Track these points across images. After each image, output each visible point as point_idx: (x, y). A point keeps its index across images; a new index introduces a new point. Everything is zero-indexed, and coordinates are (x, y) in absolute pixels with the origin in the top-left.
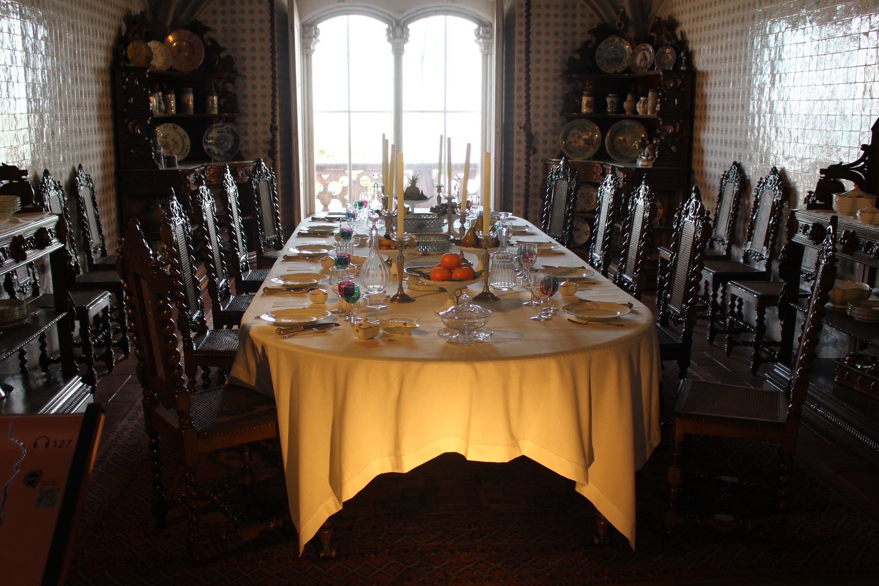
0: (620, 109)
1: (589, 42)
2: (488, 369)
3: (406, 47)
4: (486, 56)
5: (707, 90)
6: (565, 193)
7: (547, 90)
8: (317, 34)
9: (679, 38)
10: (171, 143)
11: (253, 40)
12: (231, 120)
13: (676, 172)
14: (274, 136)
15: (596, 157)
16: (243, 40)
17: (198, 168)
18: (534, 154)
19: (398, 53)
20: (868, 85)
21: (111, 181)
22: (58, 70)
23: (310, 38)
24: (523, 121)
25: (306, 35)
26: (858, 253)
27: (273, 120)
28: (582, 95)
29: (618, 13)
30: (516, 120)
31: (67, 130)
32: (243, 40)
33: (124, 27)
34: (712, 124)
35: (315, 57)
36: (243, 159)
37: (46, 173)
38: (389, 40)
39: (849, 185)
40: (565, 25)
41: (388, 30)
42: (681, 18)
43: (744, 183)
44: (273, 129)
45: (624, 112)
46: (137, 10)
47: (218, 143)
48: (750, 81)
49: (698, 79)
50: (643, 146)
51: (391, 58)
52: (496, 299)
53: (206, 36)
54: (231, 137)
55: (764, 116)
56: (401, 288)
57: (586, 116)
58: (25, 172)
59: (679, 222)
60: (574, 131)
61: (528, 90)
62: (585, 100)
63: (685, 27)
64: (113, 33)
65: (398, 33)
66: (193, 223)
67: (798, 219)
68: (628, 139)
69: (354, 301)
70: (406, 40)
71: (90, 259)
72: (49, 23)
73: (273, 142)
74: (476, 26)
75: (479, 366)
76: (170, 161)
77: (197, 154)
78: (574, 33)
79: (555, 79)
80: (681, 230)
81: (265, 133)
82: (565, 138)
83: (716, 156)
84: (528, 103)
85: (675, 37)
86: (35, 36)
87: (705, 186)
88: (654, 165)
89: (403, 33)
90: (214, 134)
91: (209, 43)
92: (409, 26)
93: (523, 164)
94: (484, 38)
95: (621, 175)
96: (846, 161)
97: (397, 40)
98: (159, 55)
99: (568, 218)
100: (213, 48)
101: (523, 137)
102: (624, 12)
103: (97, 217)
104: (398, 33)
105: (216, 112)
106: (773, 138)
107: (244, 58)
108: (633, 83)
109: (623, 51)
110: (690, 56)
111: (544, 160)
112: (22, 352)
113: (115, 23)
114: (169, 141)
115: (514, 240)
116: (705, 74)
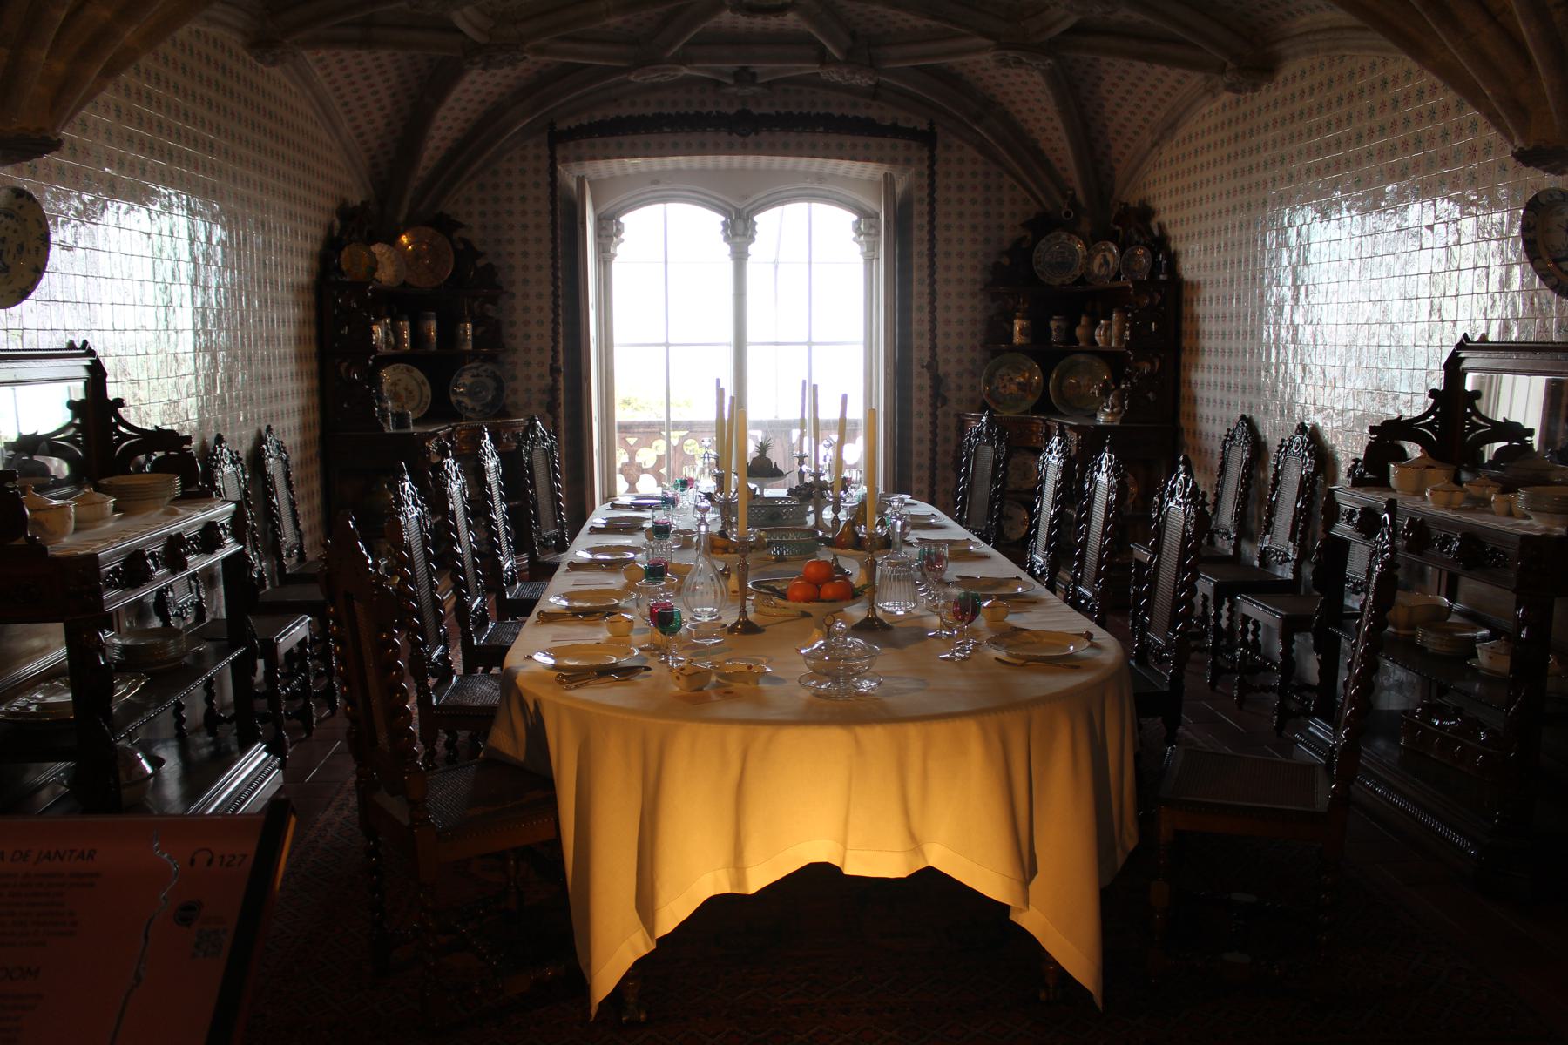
0: (1070, 338)
2: (874, 737)
3: (752, 248)
4: (869, 261)
5: (1200, 309)
6: (989, 465)
7: (961, 311)
8: (619, 231)
9: (1156, 232)
10: (403, 393)
11: (525, 240)
12: (491, 358)
13: (1155, 430)
14: (555, 381)
15: (1036, 409)
16: (511, 241)
17: (441, 429)
18: (943, 404)
19: (740, 257)
20: (1436, 301)
21: (314, 450)
22: (240, 288)
23: (610, 237)
24: (926, 356)
25: (603, 233)
26: (1429, 551)
27: (555, 359)
28: (1015, 317)
30: (915, 355)
31: (250, 376)
32: (511, 241)
33: (337, 223)
34: (1206, 360)
35: (617, 267)
36: (509, 416)
37: (219, 439)
38: (727, 239)
39: (1413, 450)
40: (987, 214)
41: (724, 224)
42: (1159, 204)
43: (1257, 447)
44: (554, 371)
45: (1077, 342)
46: (356, 199)
47: (471, 393)
48: (1262, 296)
49: (1186, 294)
50: (1105, 392)
51: (728, 266)
52: (887, 628)
53: (456, 236)
54: (491, 384)
55: (1285, 348)
56: (743, 613)
57: (1020, 349)
58: (188, 440)
59: (1161, 509)
60: (1002, 371)
61: (933, 310)
62: (1017, 325)
63: (1164, 217)
64: (320, 233)
65: (739, 230)
66: (433, 512)
67: (1340, 501)
68: (1084, 382)
69: (674, 631)
70: (752, 239)
71: (282, 567)
72: (229, 221)
73: (553, 390)
74: (855, 218)
75: (859, 730)
76: (401, 420)
77: (442, 409)
78: (1001, 227)
79: (974, 295)
80: (1165, 521)
81: (541, 377)
82: (989, 382)
83: (1215, 409)
84: (933, 330)
85: (1150, 231)
86: (209, 239)
87: (1199, 451)
89: (746, 228)
90: (467, 379)
91: (461, 246)
92: (756, 218)
93: (927, 419)
94: (867, 234)
95: (1073, 437)
96: (1408, 414)
97: (738, 240)
98: (389, 261)
99: (996, 501)
100: (467, 253)
101: (927, 382)
102: (1074, 195)
103: (292, 504)
104: (739, 230)
105: (470, 347)
106: (1299, 381)
107: (512, 267)
108: (1089, 300)
109: (1073, 252)
110: (1173, 259)
111: (958, 415)
112: (179, 707)
113: (324, 219)
114: (401, 390)
115: (913, 536)
116: (1195, 286)
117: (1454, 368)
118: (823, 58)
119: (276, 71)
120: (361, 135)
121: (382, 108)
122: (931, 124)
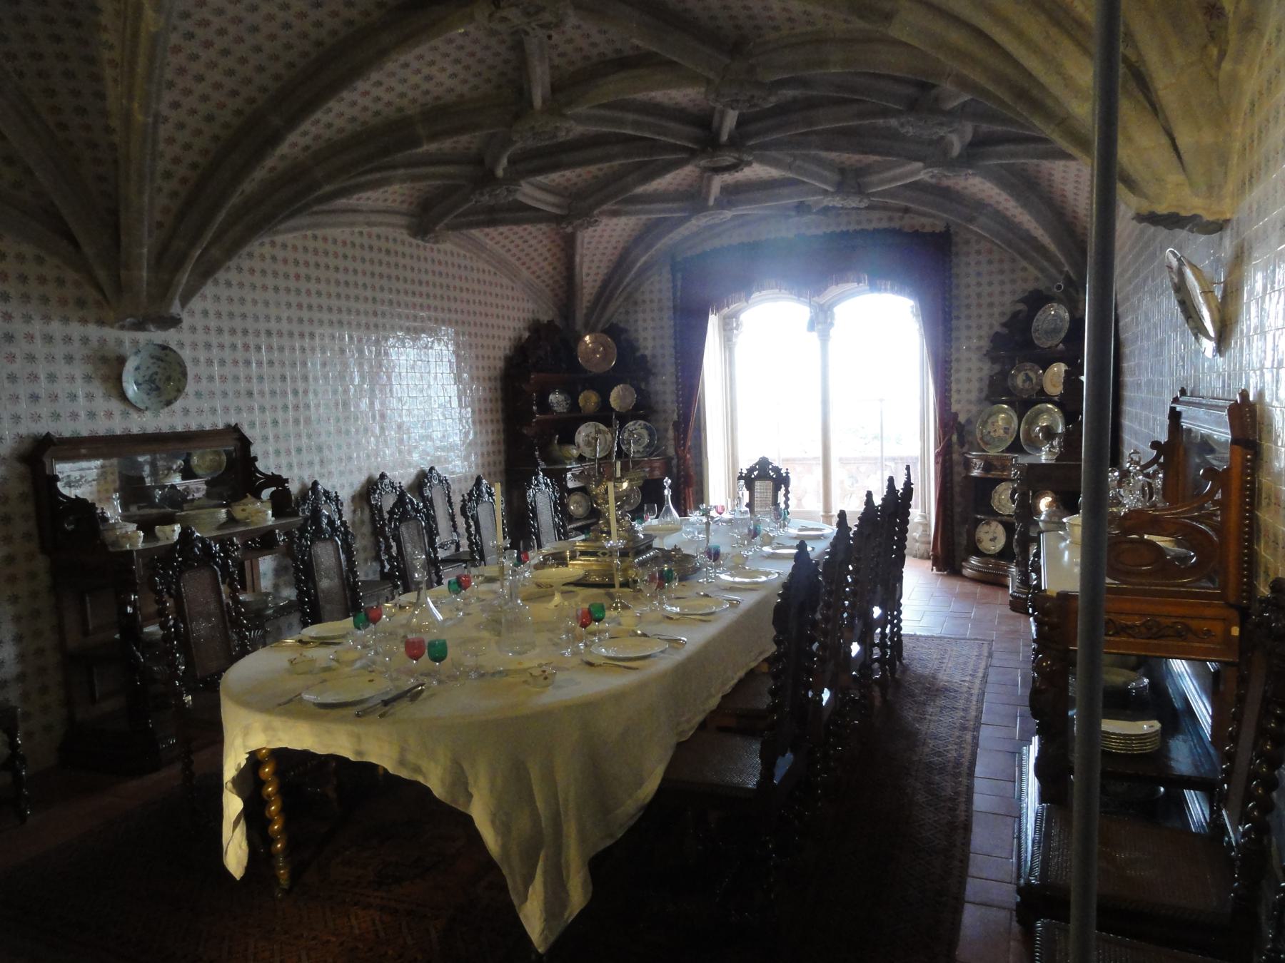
1: (1020, 312)
3: (833, 332)
7: (973, 372)
15: (1009, 450)
19: (825, 338)
23: (731, 330)
29: (1061, 272)
70: (832, 324)
88: (1057, 459)
89: (826, 318)
117: (1175, 416)
118: (825, 192)
119: (447, 246)
120: (538, 277)
121: (546, 259)
122: (948, 227)
